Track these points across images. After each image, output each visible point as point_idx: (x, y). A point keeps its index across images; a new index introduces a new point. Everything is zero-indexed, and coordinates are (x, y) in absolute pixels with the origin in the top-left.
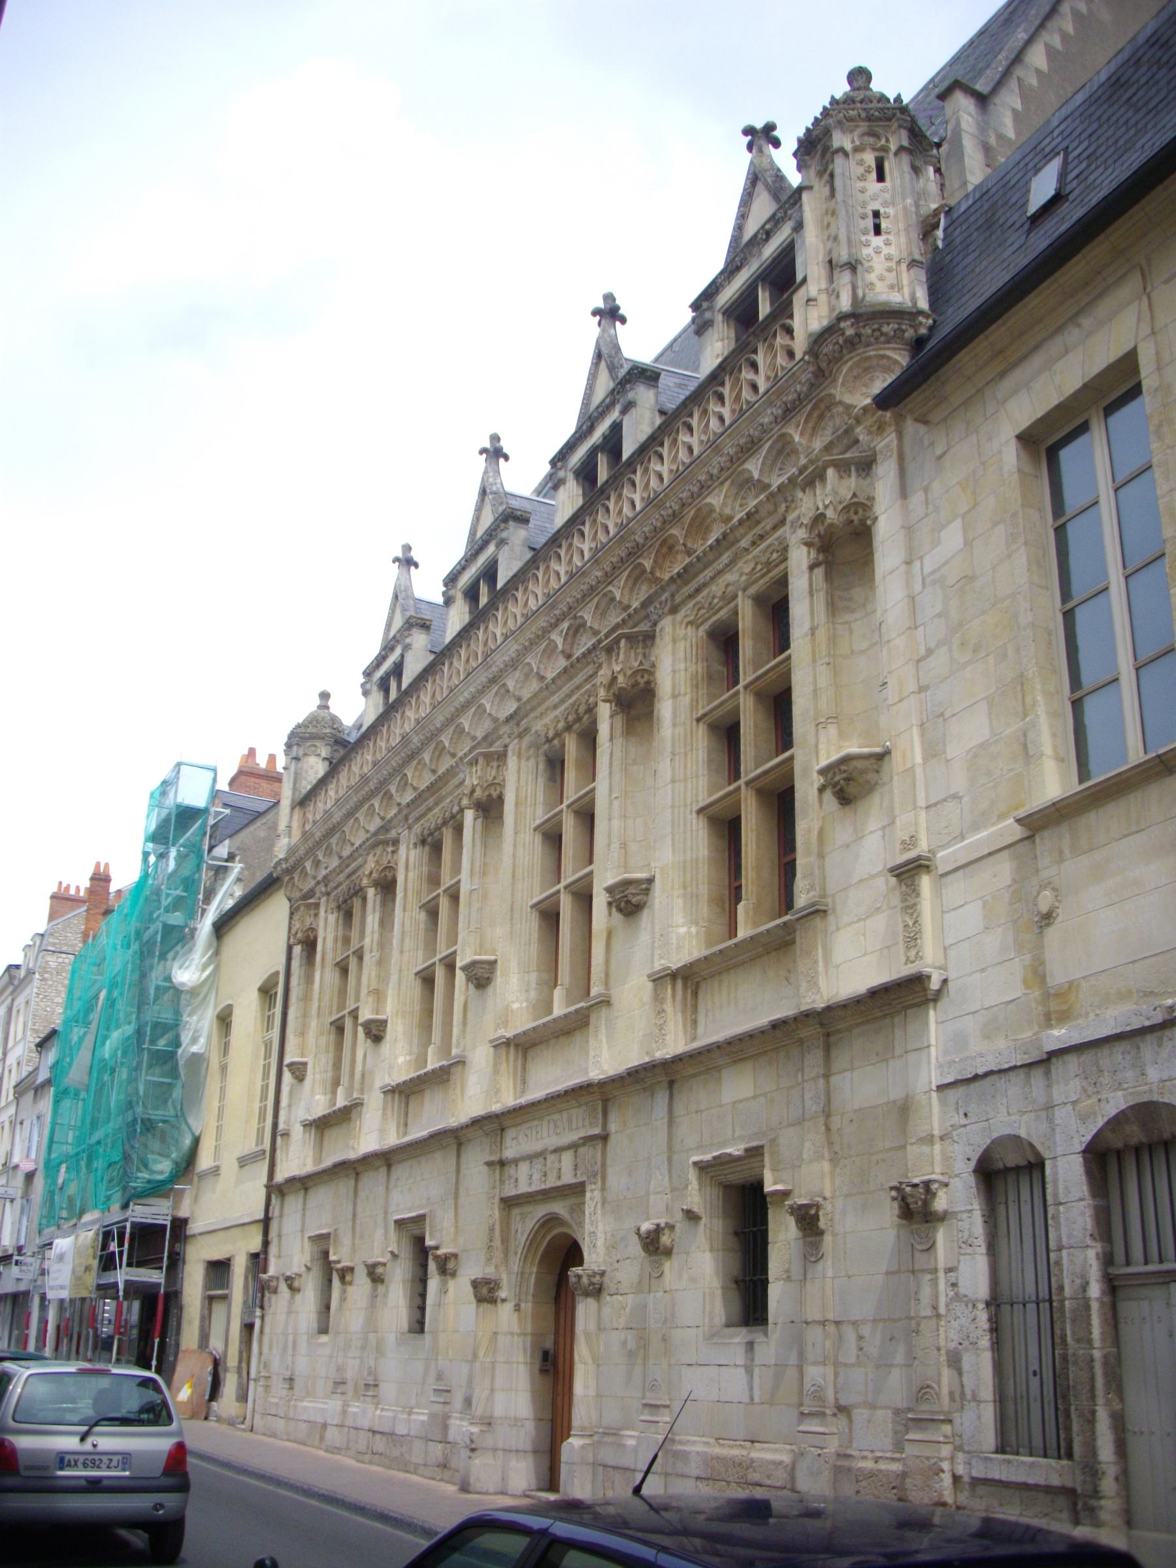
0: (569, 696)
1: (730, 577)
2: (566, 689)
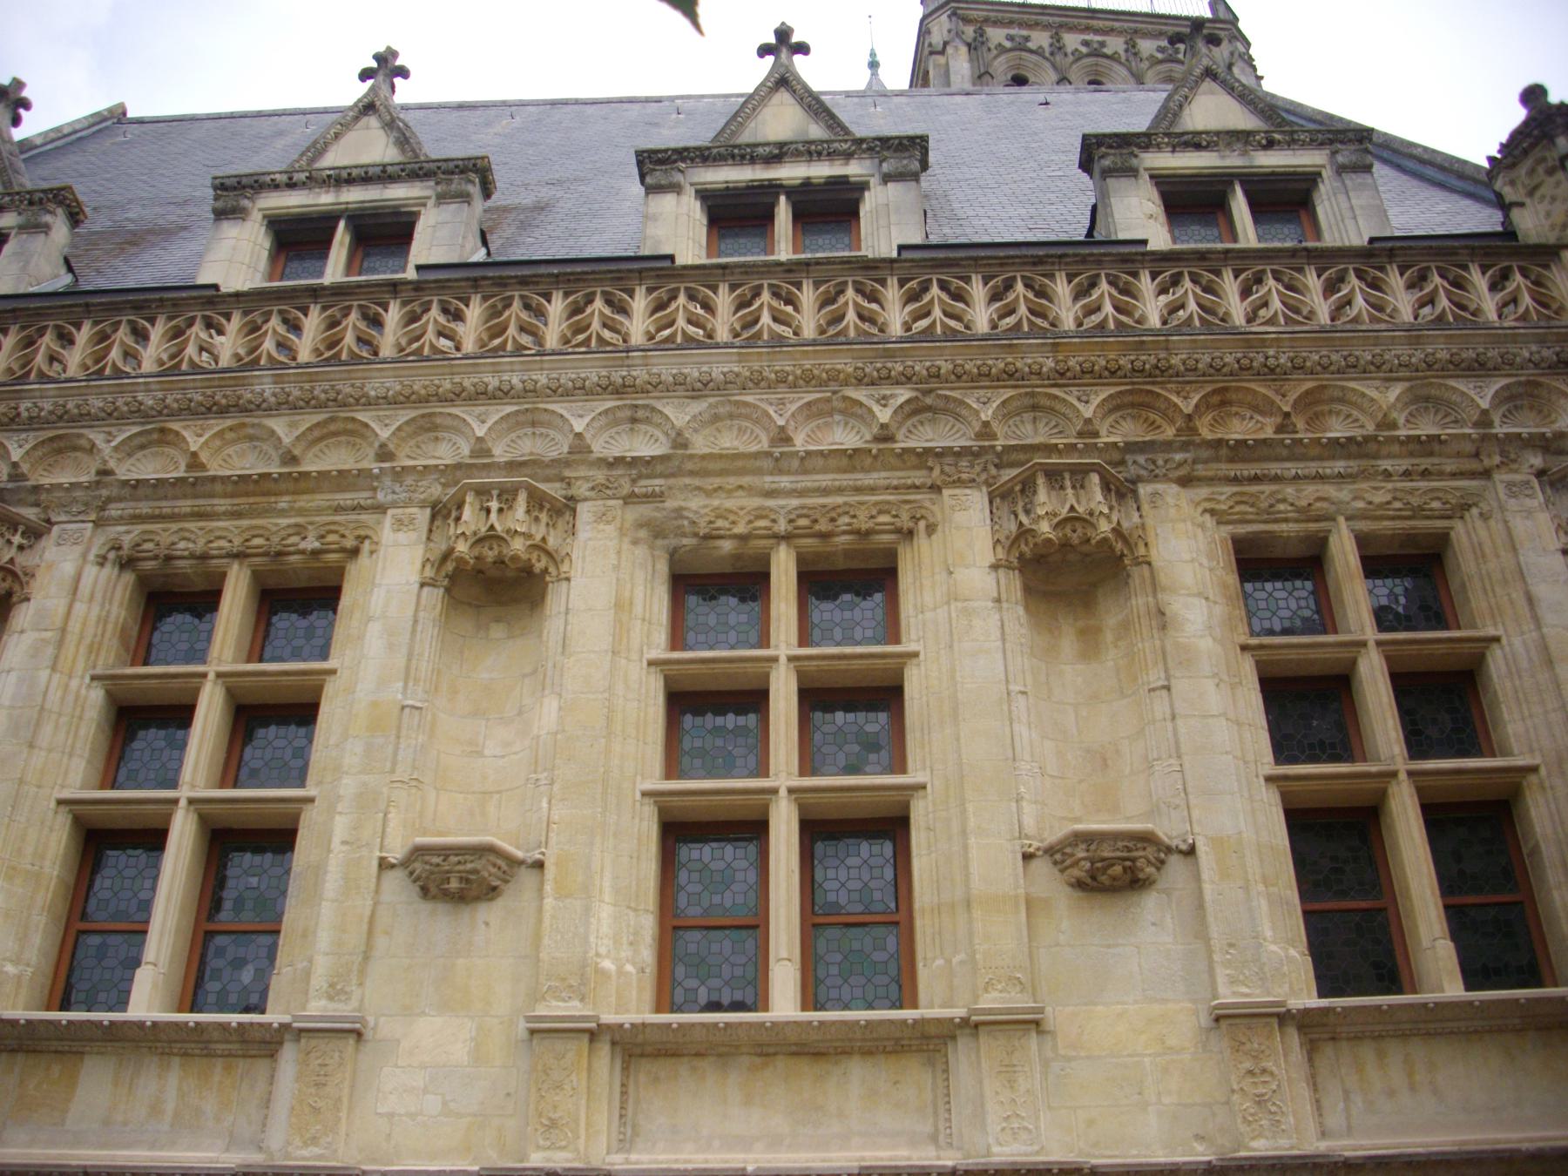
0: (825, 492)
1: (1341, 493)
2: (825, 480)
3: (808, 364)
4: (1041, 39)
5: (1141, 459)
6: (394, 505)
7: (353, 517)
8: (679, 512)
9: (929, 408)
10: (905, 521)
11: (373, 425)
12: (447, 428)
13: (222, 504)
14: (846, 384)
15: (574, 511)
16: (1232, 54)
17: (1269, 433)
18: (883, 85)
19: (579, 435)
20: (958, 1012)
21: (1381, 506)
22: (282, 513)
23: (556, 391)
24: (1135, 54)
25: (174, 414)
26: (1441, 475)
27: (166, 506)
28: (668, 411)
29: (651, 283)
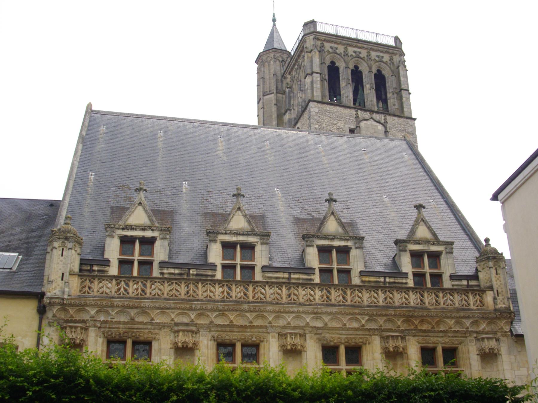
0: (351, 335)
1: (440, 339)
3: (350, 310)
4: (341, 49)
5: (407, 332)
6: (271, 332)
7: (262, 334)
8: (324, 337)
9: (371, 320)
10: (365, 342)
11: (268, 317)
12: (281, 318)
13: (236, 330)
14: (357, 315)
15: (305, 336)
16: (400, 62)
17: (430, 328)
18: (285, 48)
19: (308, 323)
21: (447, 342)
22: (248, 332)
23: (303, 312)
24: (370, 59)
25: (226, 311)
26: (458, 337)
27: (224, 329)
28: (324, 318)
29: (319, 286)
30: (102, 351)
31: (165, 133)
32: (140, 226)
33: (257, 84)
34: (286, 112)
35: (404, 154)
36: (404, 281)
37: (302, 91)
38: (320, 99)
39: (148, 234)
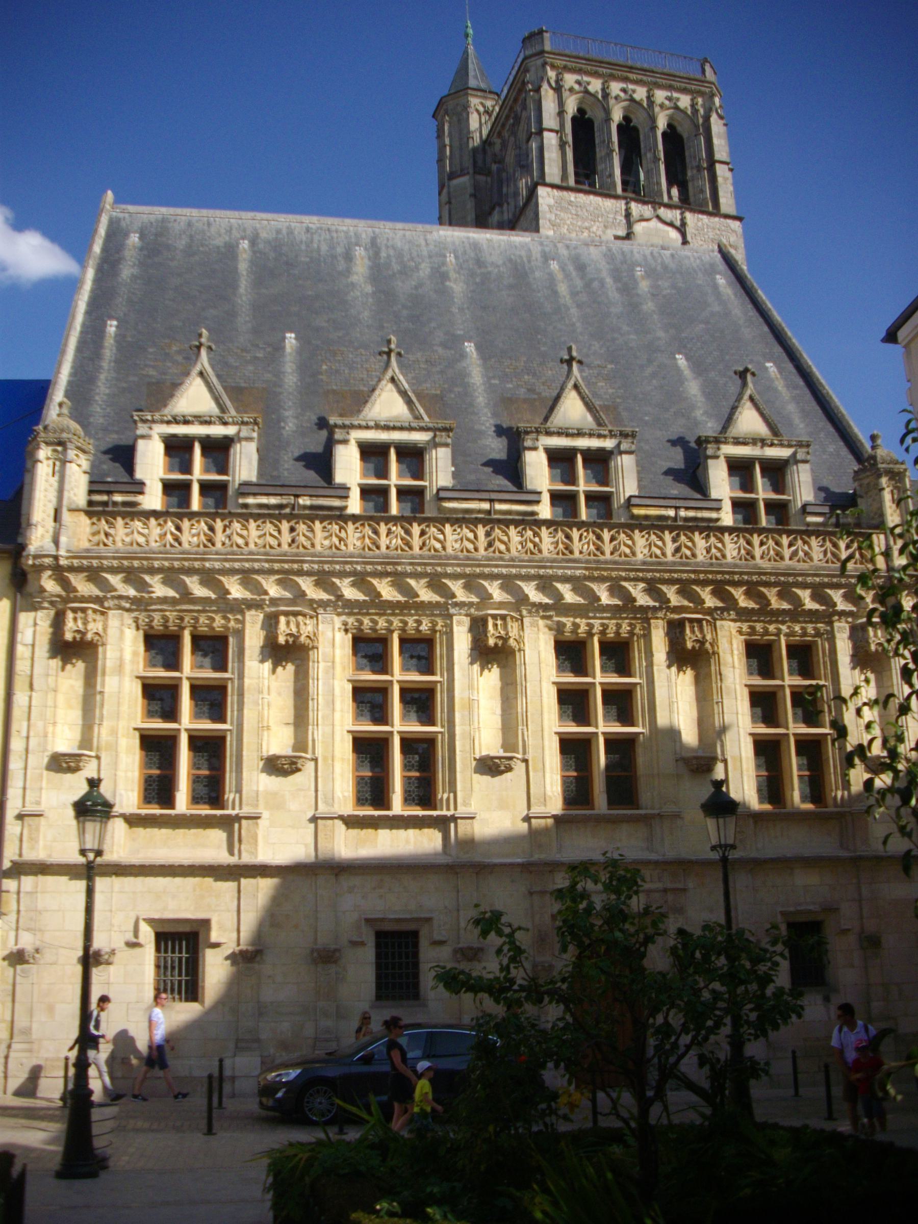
15: (522, 621)
20: (656, 812)
30: (135, 654)
31: (253, 242)
32: (200, 417)
33: (436, 158)
34: (493, 209)
35: (718, 277)
36: (714, 515)
37: (522, 167)
38: (557, 180)
39: (217, 430)
